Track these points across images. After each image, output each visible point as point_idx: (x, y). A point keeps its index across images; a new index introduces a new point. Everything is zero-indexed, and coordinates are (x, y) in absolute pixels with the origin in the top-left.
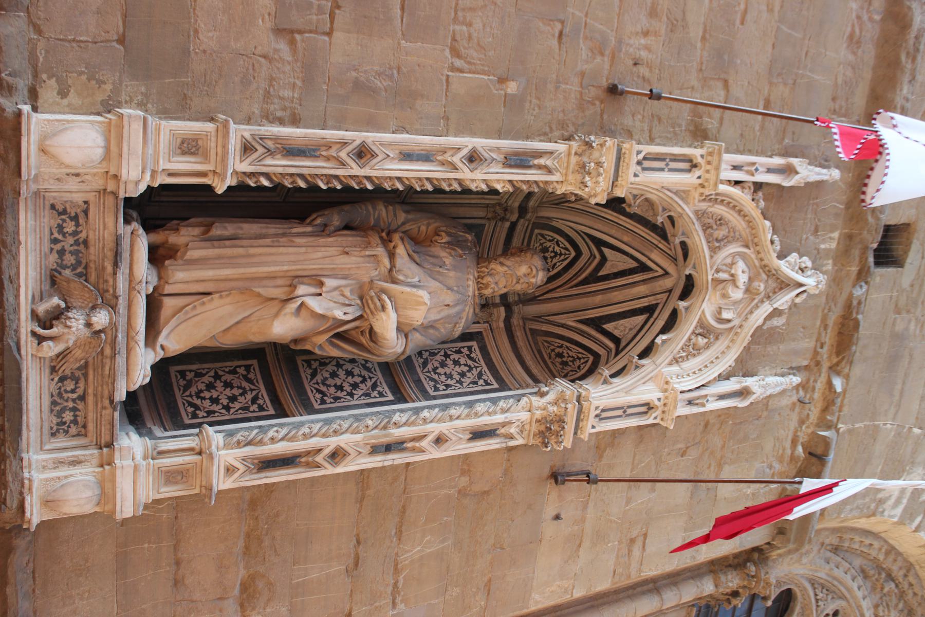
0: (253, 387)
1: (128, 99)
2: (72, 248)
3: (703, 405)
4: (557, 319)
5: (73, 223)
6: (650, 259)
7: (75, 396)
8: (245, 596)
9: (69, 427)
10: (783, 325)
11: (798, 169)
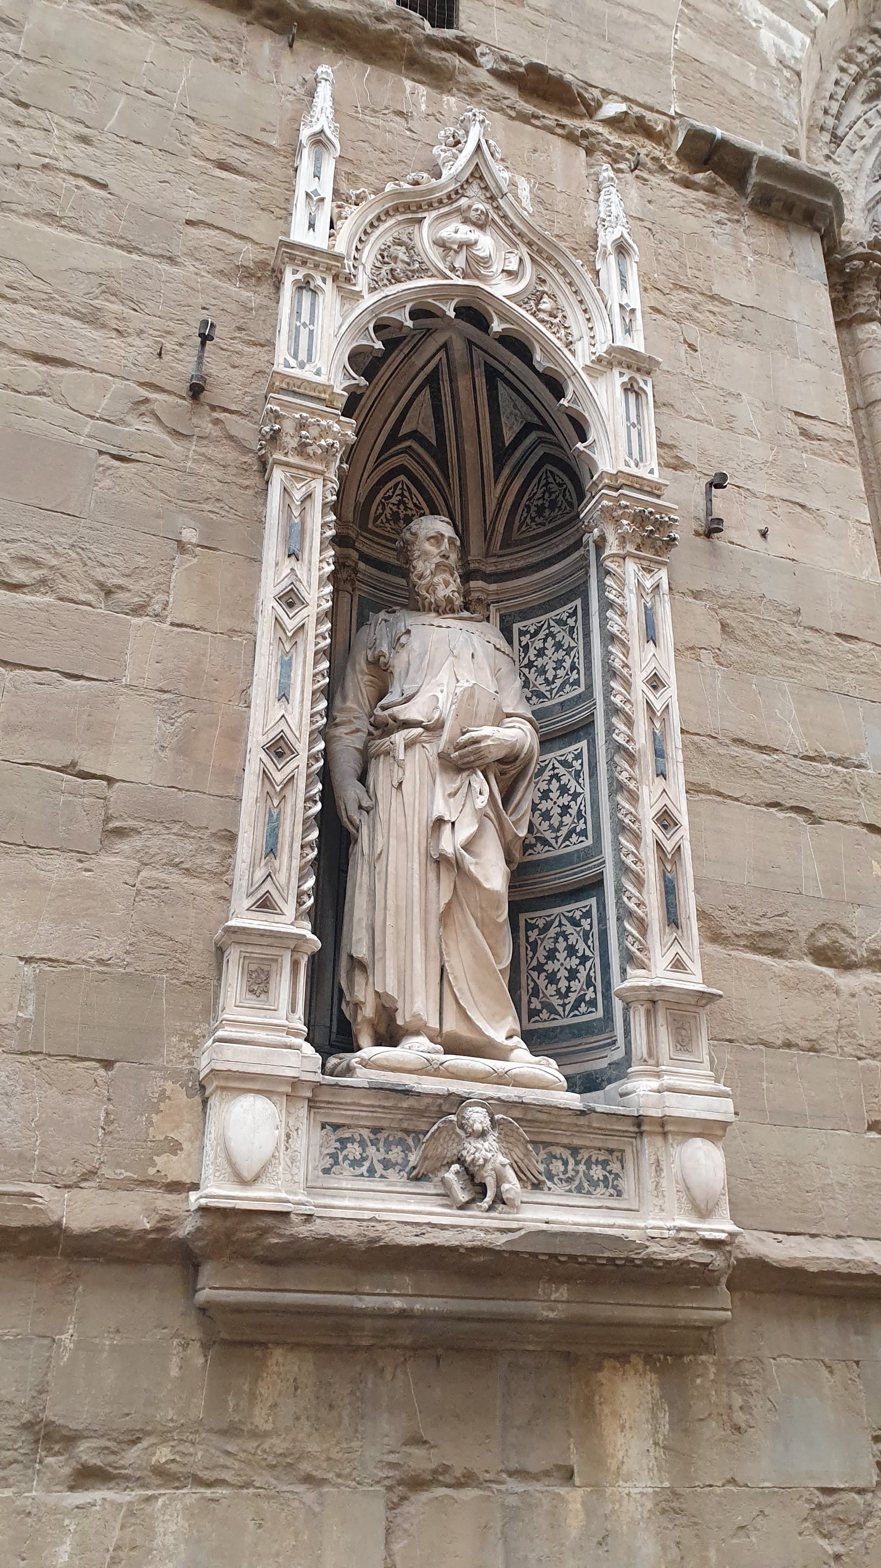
0: (556, 923)
1: (186, 1061)
4: (491, 507)
5: (349, 1145)
7: (571, 1161)
9: (610, 1172)
11: (317, 129)
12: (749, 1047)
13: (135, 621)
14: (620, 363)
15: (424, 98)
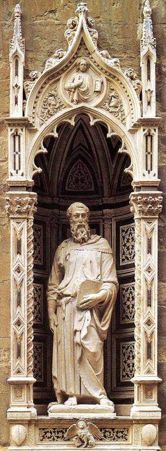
4: (112, 173)
11: (14, 51)
14: (143, 125)
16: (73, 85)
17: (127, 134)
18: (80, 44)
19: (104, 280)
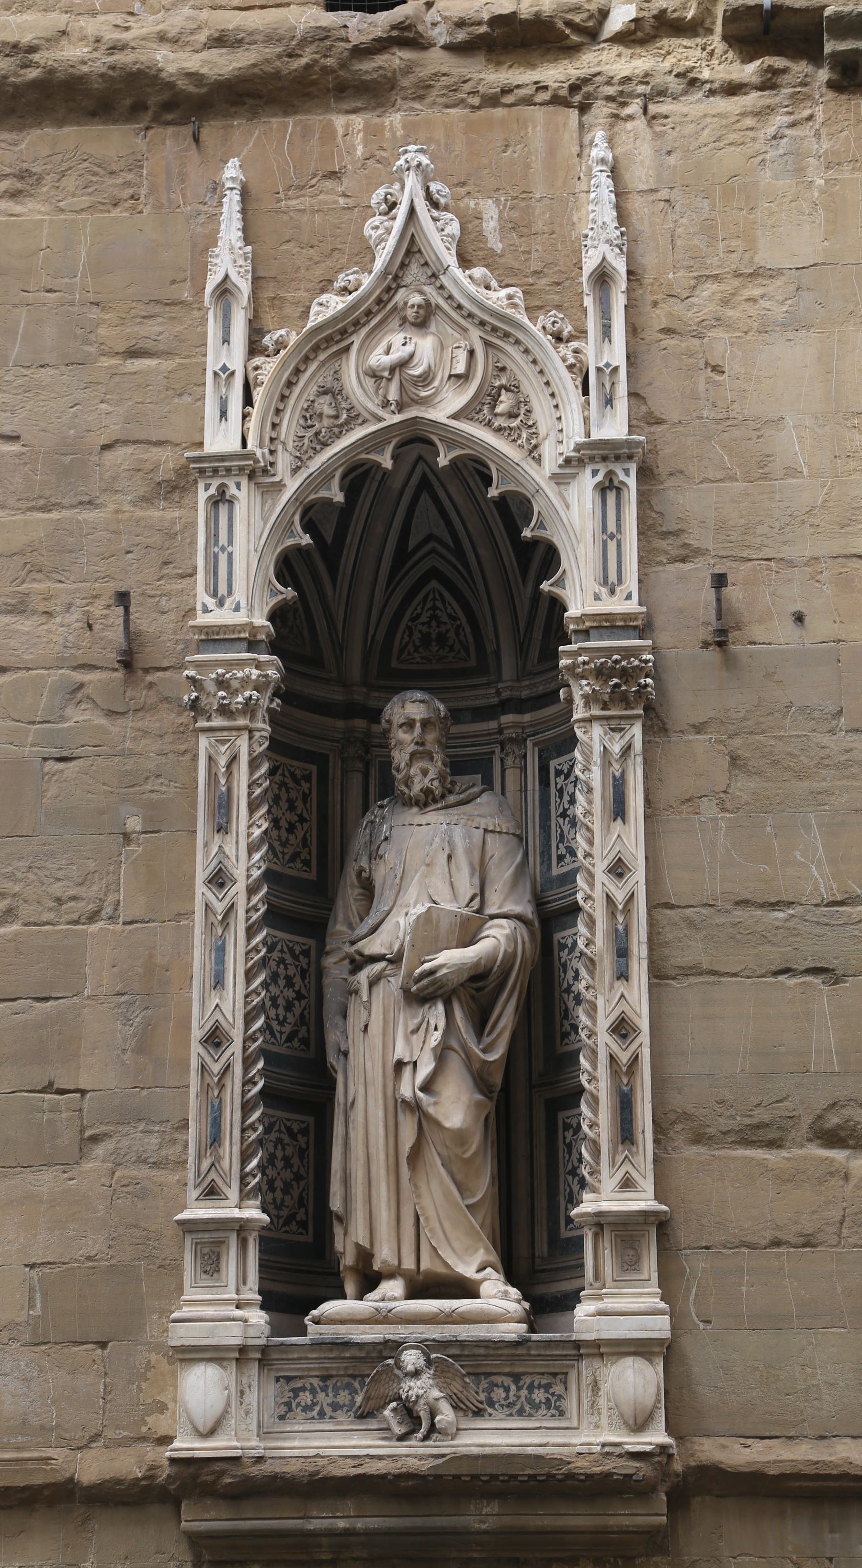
2: (330, 1395)
3: (616, 369)
5: (301, 1394)
6: (406, 484)
7: (513, 1388)
8: (851, 1142)
9: (553, 1394)
10: (497, 202)
11: (219, 277)
12: (730, 1252)
13: (94, 928)
14: (592, 459)
15: (361, 135)
16: (387, 360)
17: (550, 489)
18: (409, 253)
19: (491, 910)
